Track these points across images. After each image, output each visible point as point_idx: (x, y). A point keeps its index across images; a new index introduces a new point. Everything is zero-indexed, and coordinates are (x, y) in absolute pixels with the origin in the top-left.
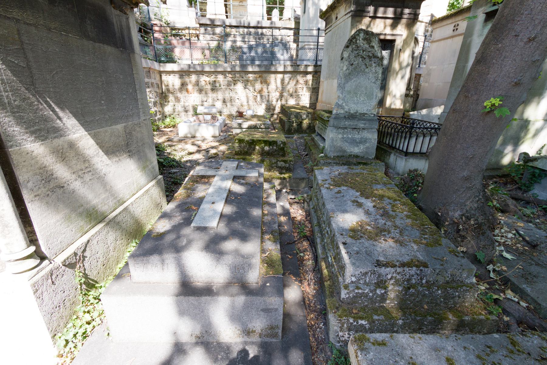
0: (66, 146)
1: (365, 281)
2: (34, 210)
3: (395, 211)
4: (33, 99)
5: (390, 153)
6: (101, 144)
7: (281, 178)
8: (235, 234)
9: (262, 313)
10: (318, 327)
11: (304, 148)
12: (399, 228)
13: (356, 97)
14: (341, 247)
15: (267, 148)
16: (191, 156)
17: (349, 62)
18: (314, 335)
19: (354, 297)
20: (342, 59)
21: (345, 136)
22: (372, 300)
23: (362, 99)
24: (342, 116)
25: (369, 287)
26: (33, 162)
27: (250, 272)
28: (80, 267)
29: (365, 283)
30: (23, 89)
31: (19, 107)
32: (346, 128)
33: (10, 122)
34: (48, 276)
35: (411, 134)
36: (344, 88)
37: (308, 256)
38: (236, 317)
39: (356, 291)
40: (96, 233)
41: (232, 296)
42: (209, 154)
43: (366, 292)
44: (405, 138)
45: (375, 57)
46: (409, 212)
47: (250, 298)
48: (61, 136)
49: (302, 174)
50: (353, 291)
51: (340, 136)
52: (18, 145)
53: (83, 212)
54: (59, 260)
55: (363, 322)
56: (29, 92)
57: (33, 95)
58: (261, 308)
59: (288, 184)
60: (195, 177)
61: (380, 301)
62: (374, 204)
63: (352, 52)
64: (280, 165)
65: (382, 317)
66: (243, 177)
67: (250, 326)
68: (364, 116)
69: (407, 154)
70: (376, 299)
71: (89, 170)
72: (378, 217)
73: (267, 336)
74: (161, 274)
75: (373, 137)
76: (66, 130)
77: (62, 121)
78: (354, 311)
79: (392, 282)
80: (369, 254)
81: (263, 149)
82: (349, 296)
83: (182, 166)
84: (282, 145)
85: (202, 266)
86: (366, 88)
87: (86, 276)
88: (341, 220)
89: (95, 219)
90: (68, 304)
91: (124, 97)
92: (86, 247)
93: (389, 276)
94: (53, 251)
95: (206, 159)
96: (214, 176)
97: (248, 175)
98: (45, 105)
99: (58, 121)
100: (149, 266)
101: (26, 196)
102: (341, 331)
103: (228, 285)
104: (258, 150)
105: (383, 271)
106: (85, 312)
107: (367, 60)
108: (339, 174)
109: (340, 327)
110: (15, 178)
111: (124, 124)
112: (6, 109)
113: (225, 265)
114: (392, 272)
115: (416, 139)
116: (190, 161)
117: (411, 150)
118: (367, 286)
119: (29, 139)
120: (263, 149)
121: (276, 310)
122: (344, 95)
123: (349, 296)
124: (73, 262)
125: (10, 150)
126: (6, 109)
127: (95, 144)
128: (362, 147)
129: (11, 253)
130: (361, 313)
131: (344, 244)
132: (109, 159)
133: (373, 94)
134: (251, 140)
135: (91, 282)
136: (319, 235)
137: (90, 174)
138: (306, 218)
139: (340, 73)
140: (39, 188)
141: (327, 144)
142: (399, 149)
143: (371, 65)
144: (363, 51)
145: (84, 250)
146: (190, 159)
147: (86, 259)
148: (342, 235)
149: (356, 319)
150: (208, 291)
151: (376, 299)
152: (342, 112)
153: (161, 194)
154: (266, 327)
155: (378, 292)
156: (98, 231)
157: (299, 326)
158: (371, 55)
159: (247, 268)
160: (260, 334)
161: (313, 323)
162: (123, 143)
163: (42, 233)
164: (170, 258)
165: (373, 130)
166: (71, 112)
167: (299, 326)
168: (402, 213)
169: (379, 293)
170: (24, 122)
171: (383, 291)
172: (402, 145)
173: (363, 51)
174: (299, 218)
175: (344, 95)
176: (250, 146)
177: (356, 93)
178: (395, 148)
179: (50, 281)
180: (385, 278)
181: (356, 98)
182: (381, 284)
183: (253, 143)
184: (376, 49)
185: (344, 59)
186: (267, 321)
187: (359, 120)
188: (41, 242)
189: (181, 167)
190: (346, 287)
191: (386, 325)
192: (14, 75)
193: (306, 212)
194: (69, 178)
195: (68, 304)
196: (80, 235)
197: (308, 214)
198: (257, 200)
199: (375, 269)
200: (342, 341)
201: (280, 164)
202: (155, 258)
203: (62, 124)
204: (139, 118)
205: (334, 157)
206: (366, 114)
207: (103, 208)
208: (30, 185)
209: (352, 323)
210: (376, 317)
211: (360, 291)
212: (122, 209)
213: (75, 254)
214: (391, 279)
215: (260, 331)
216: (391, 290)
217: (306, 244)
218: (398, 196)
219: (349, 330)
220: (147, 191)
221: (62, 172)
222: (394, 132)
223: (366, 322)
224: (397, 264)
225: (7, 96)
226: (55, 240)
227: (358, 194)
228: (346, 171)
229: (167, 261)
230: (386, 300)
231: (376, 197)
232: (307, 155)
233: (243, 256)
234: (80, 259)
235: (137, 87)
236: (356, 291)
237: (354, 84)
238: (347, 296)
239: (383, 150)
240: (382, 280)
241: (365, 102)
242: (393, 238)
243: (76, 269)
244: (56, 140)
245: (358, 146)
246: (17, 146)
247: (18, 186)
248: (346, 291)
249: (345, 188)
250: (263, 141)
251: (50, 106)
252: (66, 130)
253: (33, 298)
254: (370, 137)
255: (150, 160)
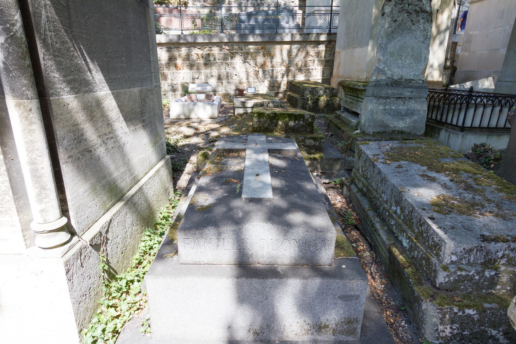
0: (94, 104)
1: (469, 260)
2: (67, 171)
3: (480, 185)
4: (70, 45)
5: (440, 130)
6: (121, 107)
7: (311, 159)
8: (294, 207)
9: (340, 302)
10: (400, 326)
11: (326, 128)
12: (494, 202)
13: (401, 59)
14: (430, 222)
15: (292, 123)
16: (188, 140)
17: (392, 18)
18: (397, 335)
19: (455, 280)
20: (383, 15)
21: (387, 107)
22: (478, 286)
23: (408, 62)
24: (383, 83)
25: (474, 268)
26: (68, 116)
27: (323, 249)
28: (104, 250)
29: (469, 263)
30: (63, 31)
31: (59, 50)
32: (388, 98)
33: (52, 66)
34: (78, 255)
35: (468, 103)
36: (386, 49)
37: (363, 246)
38: (307, 306)
39: (459, 273)
40: (117, 212)
41: (304, 278)
42: (210, 137)
43: (471, 274)
44: (460, 110)
45: (423, 11)
46: (498, 185)
47: (326, 280)
48: (91, 91)
49: (335, 154)
50: (455, 273)
51: (381, 107)
52: (57, 94)
53: (106, 185)
54: (88, 237)
55: (471, 312)
56: (67, 36)
57: (70, 39)
58: (339, 294)
59: (319, 166)
60: (221, 151)
61: (488, 286)
62: (449, 178)
63: (395, 6)
64: (308, 144)
65: (494, 305)
66: (279, 151)
67: (323, 320)
68: (410, 82)
69: (463, 129)
70: (483, 284)
71: (111, 135)
72: (461, 191)
73: (342, 332)
74: (213, 251)
75: (421, 108)
76: (95, 85)
77: (91, 74)
78: (457, 299)
79: (503, 261)
80: (469, 229)
81: (286, 124)
82: (449, 280)
83: (179, 151)
84: (310, 120)
85: (266, 242)
86: (413, 49)
87: (108, 263)
88: (416, 195)
89: (116, 195)
90: (93, 294)
91: (140, 56)
92: (109, 227)
93: (500, 254)
94: (80, 226)
95: (206, 144)
96: (244, 150)
97: (285, 148)
98: (79, 53)
99: (89, 73)
100: (202, 242)
101: (62, 156)
102: (441, 323)
103: (295, 268)
104: (282, 125)
105: (492, 246)
106: (108, 306)
107: (414, 15)
108: (391, 149)
109: (441, 319)
110: (53, 132)
111: (139, 88)
112: (49, 51)
113: (293, 241)
114: (504, 248)
115: (475, 110)
116: (188, 145)
117: (468, 124)
118: (472, 266)
119: (66, 89)
120: (286, 124)
121: (358, 297)
122: (386, 57)
123: (449, 280)
124: (98, 243)
125: (51, 98)
126: (49, 51)
127: (117, 107)
128: (408, 120)
129: (45, 222)
130: (466, 302)
131: (432, 218)
132: (128, 126)
133: (421, 56)
134: (273, 113)
135: (112, 271)
136: (377, 219)
137: (112, 140)
138: (348, 205)
139: (380, 31)
140: (72, 148)
141: (363, 119)
142: (451, 124)
143: (419, 22)
144: (409, 5)
145: (107, 232)
146: (187, 143)
147: (109, 242)
148: (424, 209)
149: (462, 308)
150: (271, 273)
151: (483, 284)
152: (384, 78)
153: (169, 178)
154: (343, 320)
155: (487, 274)
156: (119, 211)
157: (376, 324)
158: (418, 9)
159: (319, 245)
160: (334, 330)
161: (392, 321)
162: (139, 110)
163: (73, 203)
164: (228, 230)
165: (422, 100)
166: (99, 65)
167: (376, 324)
168: (490, 186)
169: (488, 276)
170: (63, 69)
171: (493, 273)
172: (457, 118)
173: (409, 5)
174: (339, 205)
175: (386, 57)
176: (271, 120)
177: (401, 55)
178: (446, 123)
179: (79, 261)
180: (494, 257)
181: (400, 61)
182: (490, 263)
183: (275, 117)
184: (425, 3)
185: (385, 15)
186: (344, 313)
187: (405, 87)
188: (71, 213)
189: (178, 152)
190: (445, 268)
191: (501, 315)
192: (57, 14)
193: (345, 198)
194: (95, 142)
195: (93, 294)
196: (103, 212)
197: (349, 200)
198: (304, 174)
199: (483, 245)
200: (442, 338)
201: (308, 142)
202: (210, 231)
203: (91, 78)
204: (152, 84)
205: (373, 133)
206: (413, 80)
207: (123, 184)
208: (65, 142)
209: (457, 313)
210: (486, 305)
211: (464, 273)
212: (137, 189)
213: (100, 233)
214: (502, 257)
215: (334, 326)
216: (503, 271)
217: (355, 234)
218: (477, 169)
219: (452, 322)
220: (158, 171)
221: (90, 133)
222: (445, 103)
223: (475, 312)
224: (509, 238)
225: (51, 36)
226: (83, 213)
227: (425, 168)
228: (398, 145)
229: (223, 236)
230: (496, 284)
231: (449, 171)
232: (332, 136)
233: (316, 230)
234: (104, 241)
235: (151, 47)
236: (459, 273)
237: (398, 44)
238: (447, 280)
239: (433, 127)
240: (491, 259)
241: (411, 65)
242: (491, 212)
243: (100, 253)
244: (87, 94)
245: (403, 120)
246: (56, 96)
247: (55, 142)
248: (445, 273)
249: (406, 162)
250: (288, 114)
251: (83, 54)
252: (95, 85)
253: (64, 277)
254: (419, 108)
255: (160, 135)
